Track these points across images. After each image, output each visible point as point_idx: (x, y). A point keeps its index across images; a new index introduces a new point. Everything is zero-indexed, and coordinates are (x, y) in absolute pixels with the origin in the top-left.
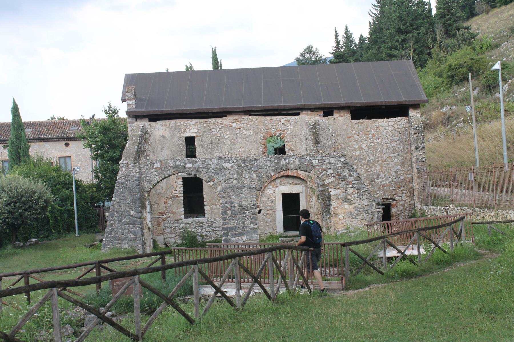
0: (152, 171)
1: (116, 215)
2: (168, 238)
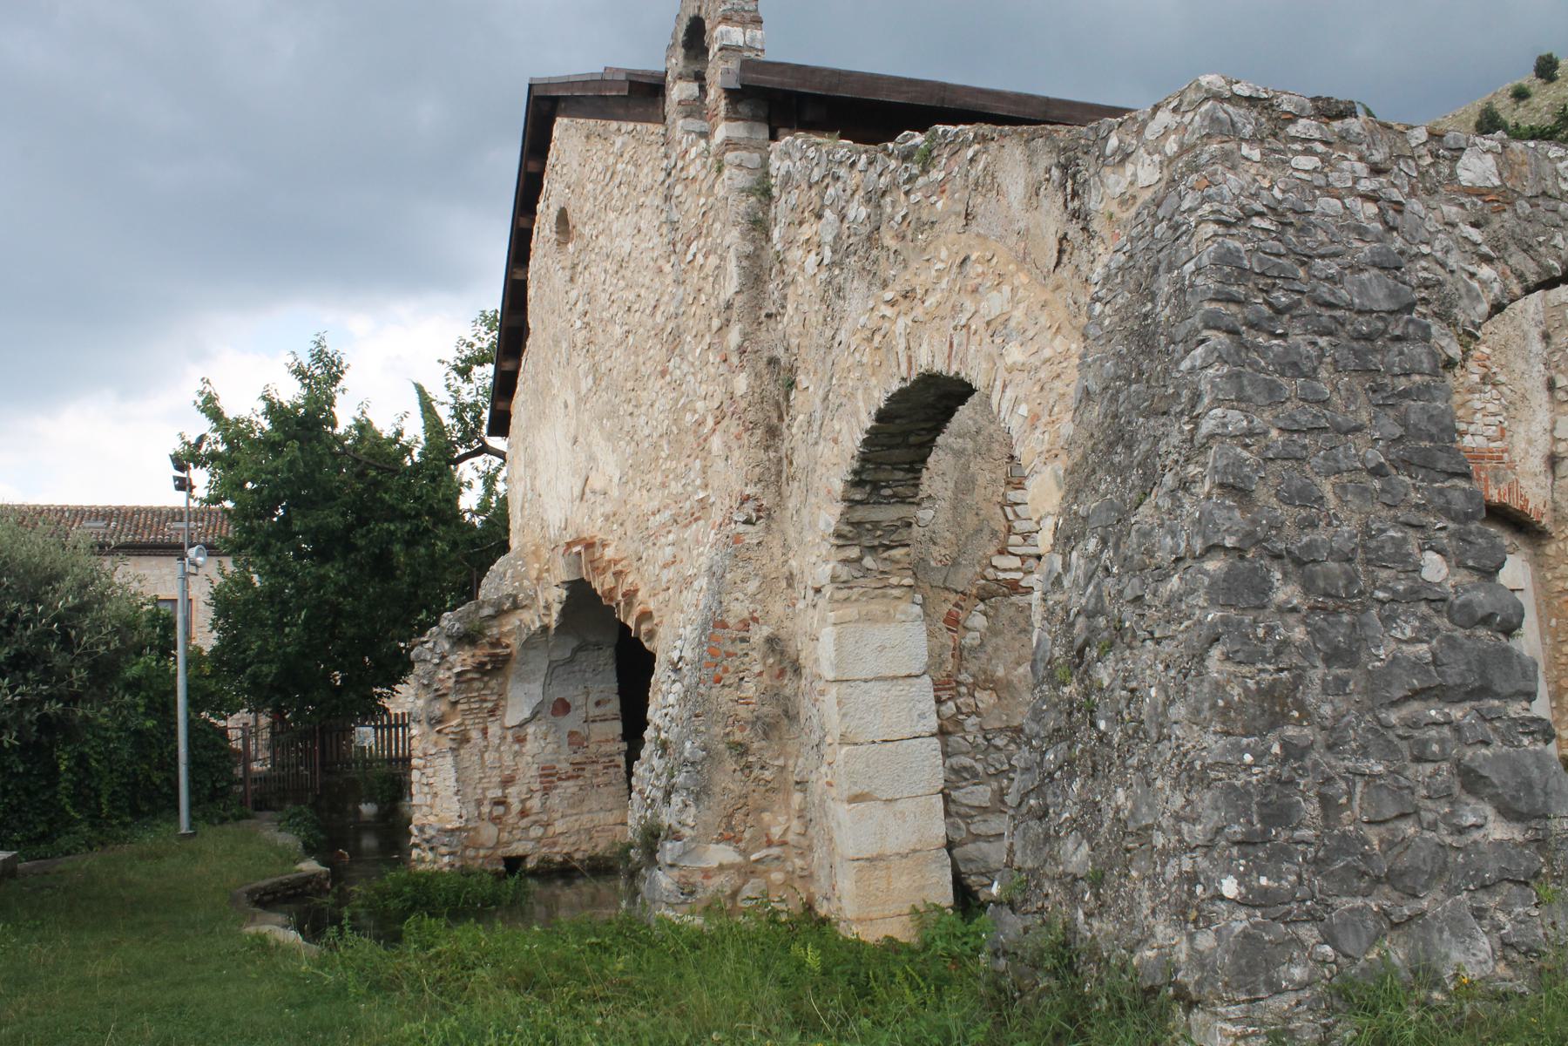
0: (1451, 211)
1: (1286, 592)
2: (977, 837)
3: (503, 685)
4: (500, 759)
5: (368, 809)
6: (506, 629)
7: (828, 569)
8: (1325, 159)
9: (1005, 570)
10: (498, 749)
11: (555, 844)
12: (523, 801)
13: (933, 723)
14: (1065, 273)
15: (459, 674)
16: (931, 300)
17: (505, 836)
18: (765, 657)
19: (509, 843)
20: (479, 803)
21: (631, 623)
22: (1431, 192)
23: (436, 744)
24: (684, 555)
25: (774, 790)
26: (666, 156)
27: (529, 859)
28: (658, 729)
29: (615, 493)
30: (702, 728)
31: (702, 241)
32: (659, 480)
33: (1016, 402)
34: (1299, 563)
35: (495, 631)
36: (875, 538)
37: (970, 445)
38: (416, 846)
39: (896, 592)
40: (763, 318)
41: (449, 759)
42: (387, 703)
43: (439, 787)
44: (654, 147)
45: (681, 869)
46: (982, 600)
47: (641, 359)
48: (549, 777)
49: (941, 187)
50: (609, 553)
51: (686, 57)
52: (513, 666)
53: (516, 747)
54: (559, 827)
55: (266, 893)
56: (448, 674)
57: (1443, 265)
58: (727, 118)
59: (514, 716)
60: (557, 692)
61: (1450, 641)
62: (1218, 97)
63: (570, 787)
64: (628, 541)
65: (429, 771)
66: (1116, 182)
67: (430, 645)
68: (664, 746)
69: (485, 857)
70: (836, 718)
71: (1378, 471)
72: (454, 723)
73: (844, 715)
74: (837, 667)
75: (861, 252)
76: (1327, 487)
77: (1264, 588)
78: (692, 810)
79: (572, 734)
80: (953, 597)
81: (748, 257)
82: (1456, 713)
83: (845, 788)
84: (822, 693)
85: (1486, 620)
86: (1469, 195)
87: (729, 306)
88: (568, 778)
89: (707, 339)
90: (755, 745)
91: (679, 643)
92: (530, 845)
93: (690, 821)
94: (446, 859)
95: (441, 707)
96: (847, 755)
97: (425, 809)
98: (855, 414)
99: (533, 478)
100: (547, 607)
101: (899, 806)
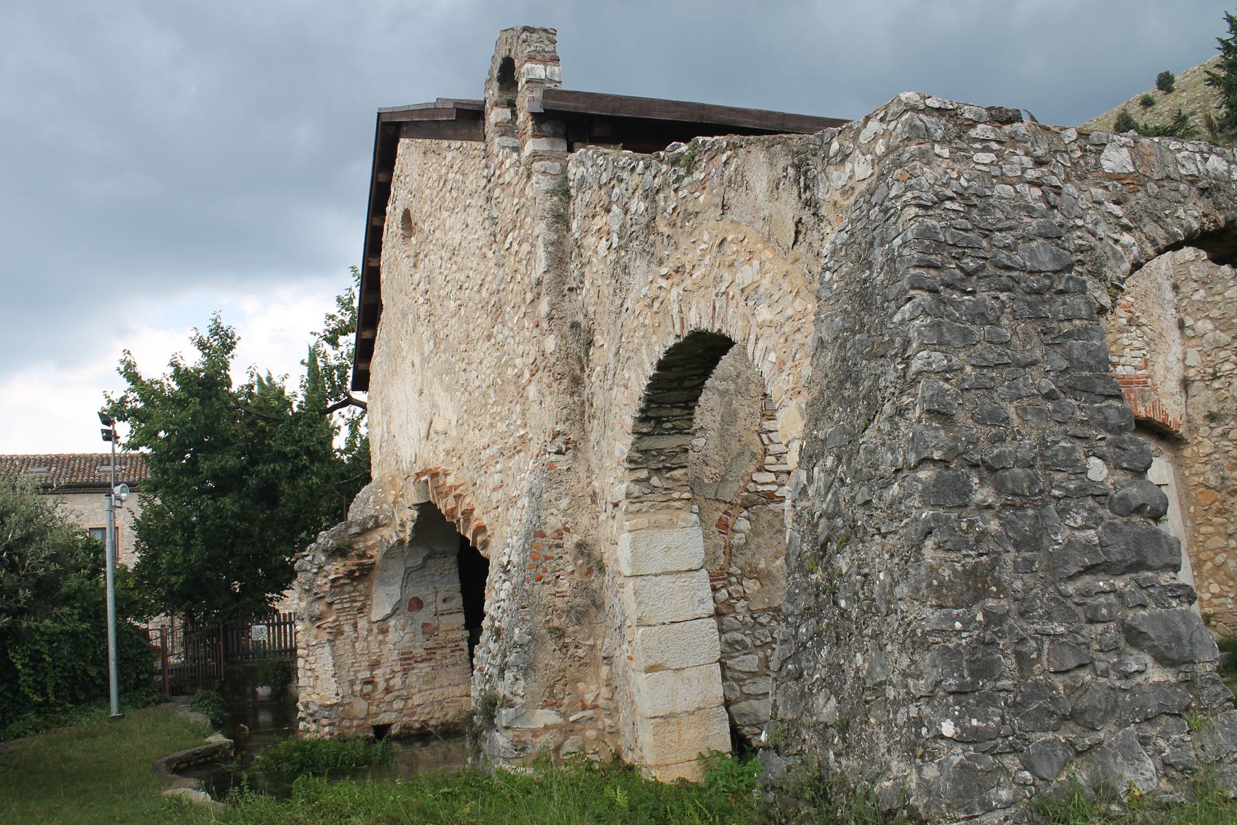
0: (1098, 192)
1: (983, 494)
2: (749, 696)
3: (369, 588)
4: (368, 647)
5: (263, 691)
6: (370, 543)
7: (623, 487)
8: (999, 155)
9: (763, 484)
10: (366, 639)
11: (414, 714)
12: (387, 680)
13: (710, 607)
14: (801, 249)
15: (333, 581)
16: (697, 274)
17: (374, 709)
18: (575, 559)
19: (377, 715)
20: (352, 683)
21: (469, 536)
22: (1082, 178)
23: (316, 637)
24: (509, 480)
25: (586, 664)
26: (487, 167)
27: (393, 727)
28: (493, 619)
29: (453, 432)
30: (528, 617)
31: (517, 232)
32: (488, 421)
33: (767, 351)
34: (992, 470)
35: (361, 545)
36: (659, 462)
37: (732, 387)
38: (302, 719)
39: (678, 504)
40: (566, 292)
41: (327, 648)
42: (277, 606)
43: (319, 672)
44: (477, 160)
45: (514, 730)
46: (746, 508)
47: (471, 327)
48: (407, 660)
49: (702, 185)
50: (450, 481)
51: (500, 89)
52: (377, 572)
53: (381, 637)
54: (416, 700)
55: (182, 762)
56: (325, 580)
57: (1094, 234)
58: (534, 136)
59: (378, 613)
60: (412, 592)
61: (1112, 528)
62: (914, 109)
63: (425, 667)
64: (465, 471)
65: (311, 659)
66: (838, 177)
67: (310, 558)
68: (498, 632)
69: (358, 726)
70: (633, 606)
71: (1050, 396)
72: (330, 620)
73: (640, 603)
74: (633, 565)
75: (641, 238)
76: (1011, 410)
77: (966, 491)
78: (522, 683)
79: (424, 625)
80: (723, 507)
81: (552, 244)
82: (1119, 583)
83: (642, 661)
84: (622, 586)
85: (1139, 510)
86: (1111, 180)
87: (539, 283)
88: (423, 661)
89: (523, 309)
90: (570, 629)
91: (507, 550)
92: (394, 716)
93: (520, 692)
94: (327, 729)
95: (319, 607)
96: (643, 634)
97: (309, 689)
98: (641, 364)
99: (389, 423)
100: (403, 525)
101: (686, 673)
